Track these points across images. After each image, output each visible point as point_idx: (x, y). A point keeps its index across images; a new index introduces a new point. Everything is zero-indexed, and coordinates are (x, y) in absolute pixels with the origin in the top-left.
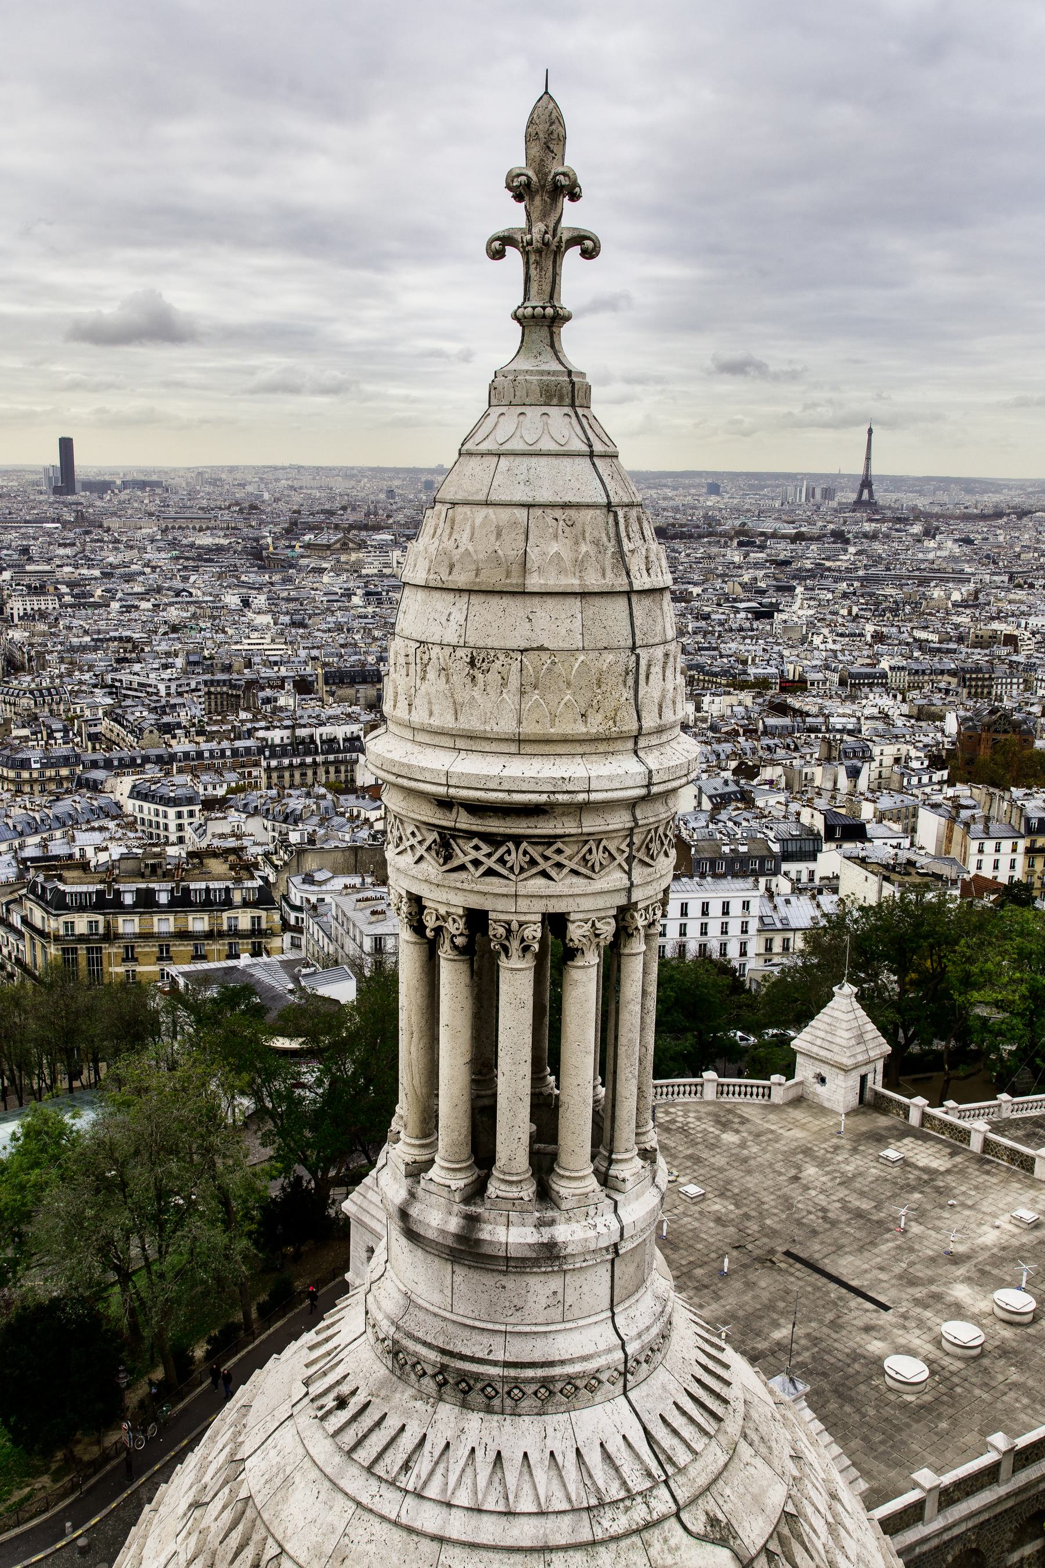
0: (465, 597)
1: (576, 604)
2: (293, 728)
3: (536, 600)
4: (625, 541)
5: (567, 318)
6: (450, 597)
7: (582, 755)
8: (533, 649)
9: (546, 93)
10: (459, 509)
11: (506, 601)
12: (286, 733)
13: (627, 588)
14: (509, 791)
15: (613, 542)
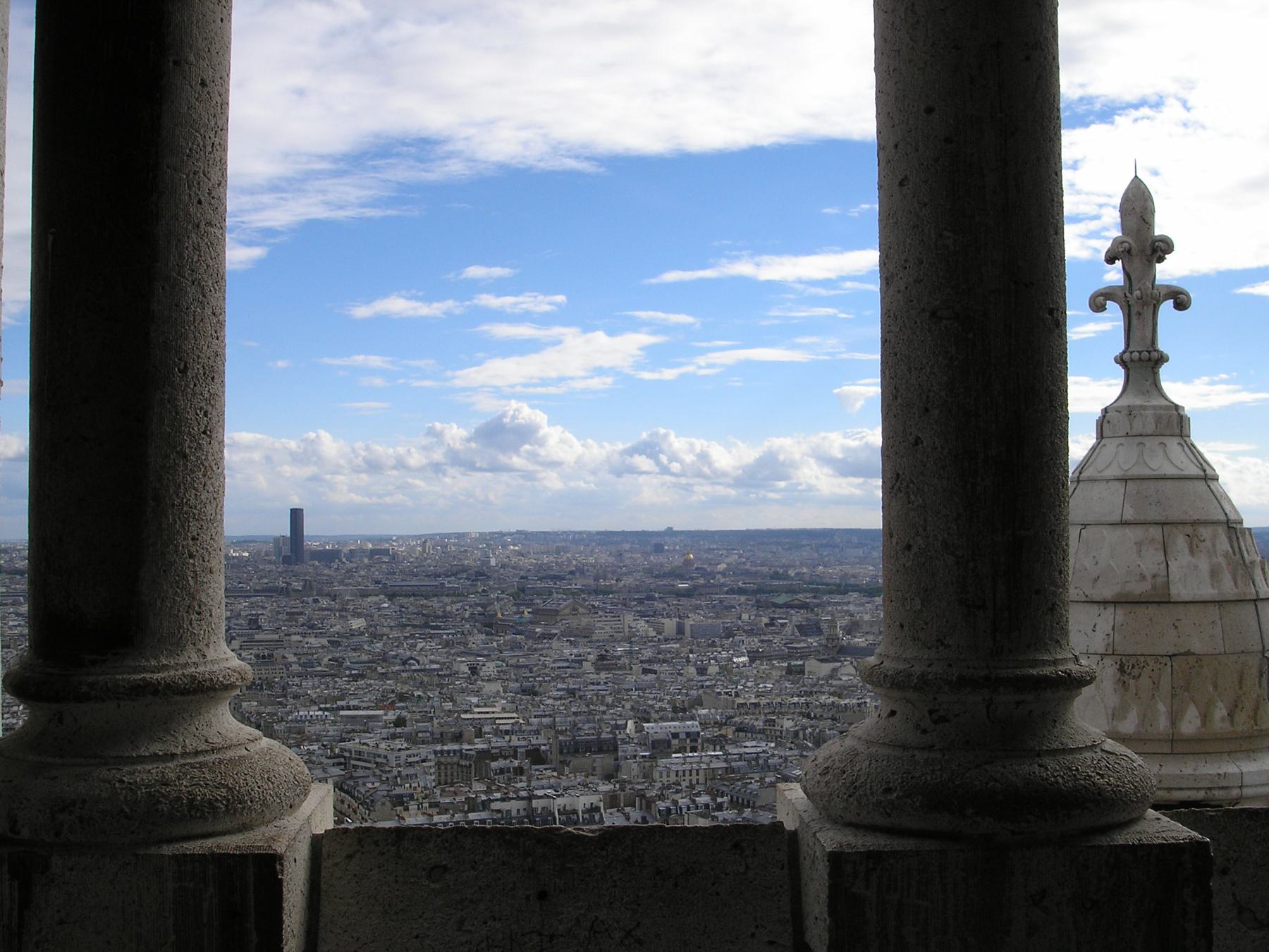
0: (1111, 609)
1: (1214, 611)
2: (530, 798)
3: (1181, 607)
4: (1245, 553)
5: (1162, 359)
6: (1095, 609)
7: (1229, 753)
8: (1181, 654)
9: (1136, 176)
10: (1090, 529)
11: (1152, 610)
12: (521, 804)
13: (1255, 598)
14: (1169, 789)
15: (1238, 556)
